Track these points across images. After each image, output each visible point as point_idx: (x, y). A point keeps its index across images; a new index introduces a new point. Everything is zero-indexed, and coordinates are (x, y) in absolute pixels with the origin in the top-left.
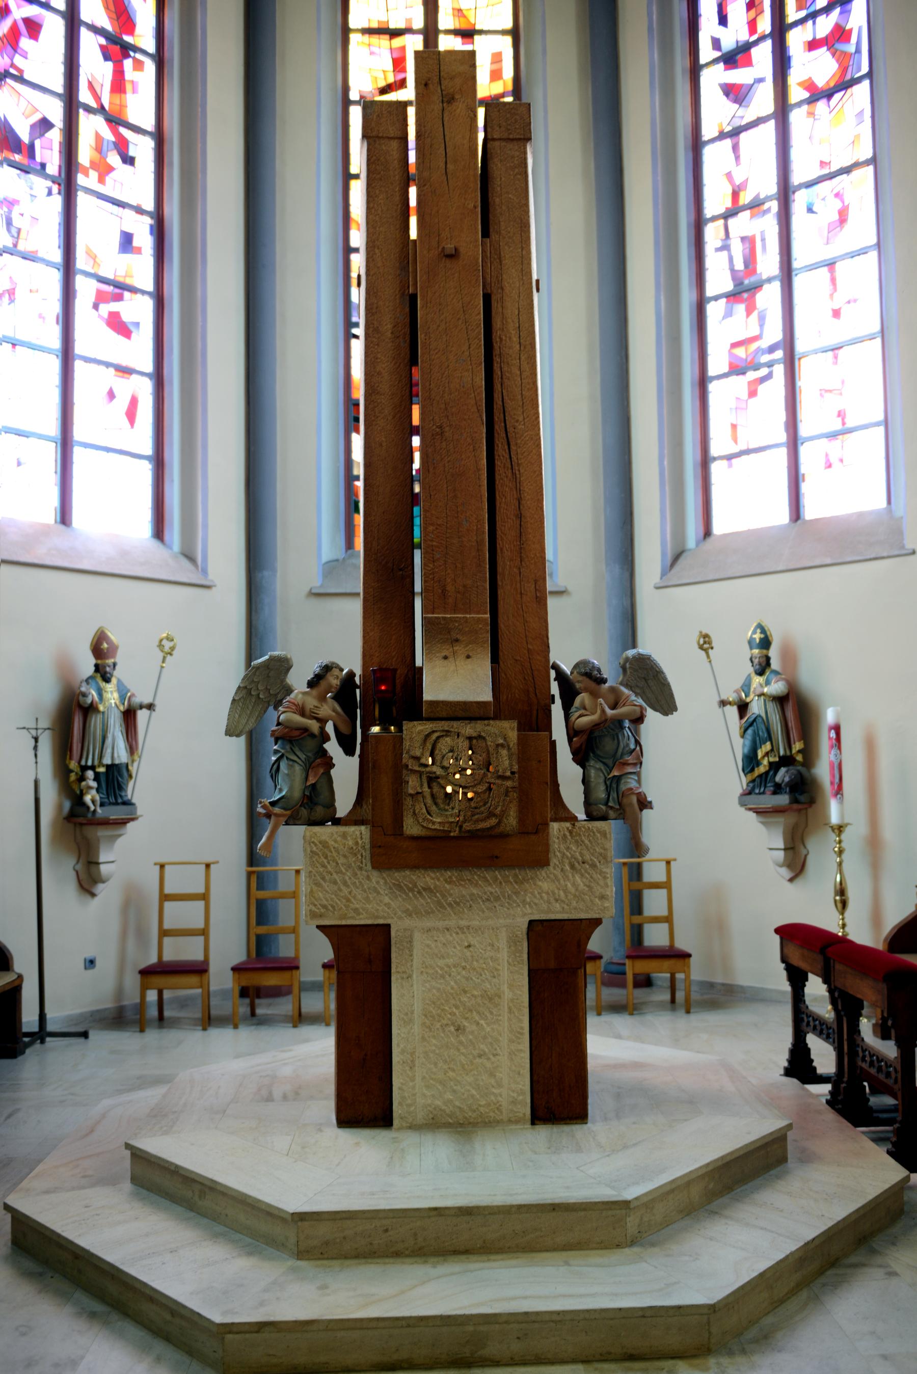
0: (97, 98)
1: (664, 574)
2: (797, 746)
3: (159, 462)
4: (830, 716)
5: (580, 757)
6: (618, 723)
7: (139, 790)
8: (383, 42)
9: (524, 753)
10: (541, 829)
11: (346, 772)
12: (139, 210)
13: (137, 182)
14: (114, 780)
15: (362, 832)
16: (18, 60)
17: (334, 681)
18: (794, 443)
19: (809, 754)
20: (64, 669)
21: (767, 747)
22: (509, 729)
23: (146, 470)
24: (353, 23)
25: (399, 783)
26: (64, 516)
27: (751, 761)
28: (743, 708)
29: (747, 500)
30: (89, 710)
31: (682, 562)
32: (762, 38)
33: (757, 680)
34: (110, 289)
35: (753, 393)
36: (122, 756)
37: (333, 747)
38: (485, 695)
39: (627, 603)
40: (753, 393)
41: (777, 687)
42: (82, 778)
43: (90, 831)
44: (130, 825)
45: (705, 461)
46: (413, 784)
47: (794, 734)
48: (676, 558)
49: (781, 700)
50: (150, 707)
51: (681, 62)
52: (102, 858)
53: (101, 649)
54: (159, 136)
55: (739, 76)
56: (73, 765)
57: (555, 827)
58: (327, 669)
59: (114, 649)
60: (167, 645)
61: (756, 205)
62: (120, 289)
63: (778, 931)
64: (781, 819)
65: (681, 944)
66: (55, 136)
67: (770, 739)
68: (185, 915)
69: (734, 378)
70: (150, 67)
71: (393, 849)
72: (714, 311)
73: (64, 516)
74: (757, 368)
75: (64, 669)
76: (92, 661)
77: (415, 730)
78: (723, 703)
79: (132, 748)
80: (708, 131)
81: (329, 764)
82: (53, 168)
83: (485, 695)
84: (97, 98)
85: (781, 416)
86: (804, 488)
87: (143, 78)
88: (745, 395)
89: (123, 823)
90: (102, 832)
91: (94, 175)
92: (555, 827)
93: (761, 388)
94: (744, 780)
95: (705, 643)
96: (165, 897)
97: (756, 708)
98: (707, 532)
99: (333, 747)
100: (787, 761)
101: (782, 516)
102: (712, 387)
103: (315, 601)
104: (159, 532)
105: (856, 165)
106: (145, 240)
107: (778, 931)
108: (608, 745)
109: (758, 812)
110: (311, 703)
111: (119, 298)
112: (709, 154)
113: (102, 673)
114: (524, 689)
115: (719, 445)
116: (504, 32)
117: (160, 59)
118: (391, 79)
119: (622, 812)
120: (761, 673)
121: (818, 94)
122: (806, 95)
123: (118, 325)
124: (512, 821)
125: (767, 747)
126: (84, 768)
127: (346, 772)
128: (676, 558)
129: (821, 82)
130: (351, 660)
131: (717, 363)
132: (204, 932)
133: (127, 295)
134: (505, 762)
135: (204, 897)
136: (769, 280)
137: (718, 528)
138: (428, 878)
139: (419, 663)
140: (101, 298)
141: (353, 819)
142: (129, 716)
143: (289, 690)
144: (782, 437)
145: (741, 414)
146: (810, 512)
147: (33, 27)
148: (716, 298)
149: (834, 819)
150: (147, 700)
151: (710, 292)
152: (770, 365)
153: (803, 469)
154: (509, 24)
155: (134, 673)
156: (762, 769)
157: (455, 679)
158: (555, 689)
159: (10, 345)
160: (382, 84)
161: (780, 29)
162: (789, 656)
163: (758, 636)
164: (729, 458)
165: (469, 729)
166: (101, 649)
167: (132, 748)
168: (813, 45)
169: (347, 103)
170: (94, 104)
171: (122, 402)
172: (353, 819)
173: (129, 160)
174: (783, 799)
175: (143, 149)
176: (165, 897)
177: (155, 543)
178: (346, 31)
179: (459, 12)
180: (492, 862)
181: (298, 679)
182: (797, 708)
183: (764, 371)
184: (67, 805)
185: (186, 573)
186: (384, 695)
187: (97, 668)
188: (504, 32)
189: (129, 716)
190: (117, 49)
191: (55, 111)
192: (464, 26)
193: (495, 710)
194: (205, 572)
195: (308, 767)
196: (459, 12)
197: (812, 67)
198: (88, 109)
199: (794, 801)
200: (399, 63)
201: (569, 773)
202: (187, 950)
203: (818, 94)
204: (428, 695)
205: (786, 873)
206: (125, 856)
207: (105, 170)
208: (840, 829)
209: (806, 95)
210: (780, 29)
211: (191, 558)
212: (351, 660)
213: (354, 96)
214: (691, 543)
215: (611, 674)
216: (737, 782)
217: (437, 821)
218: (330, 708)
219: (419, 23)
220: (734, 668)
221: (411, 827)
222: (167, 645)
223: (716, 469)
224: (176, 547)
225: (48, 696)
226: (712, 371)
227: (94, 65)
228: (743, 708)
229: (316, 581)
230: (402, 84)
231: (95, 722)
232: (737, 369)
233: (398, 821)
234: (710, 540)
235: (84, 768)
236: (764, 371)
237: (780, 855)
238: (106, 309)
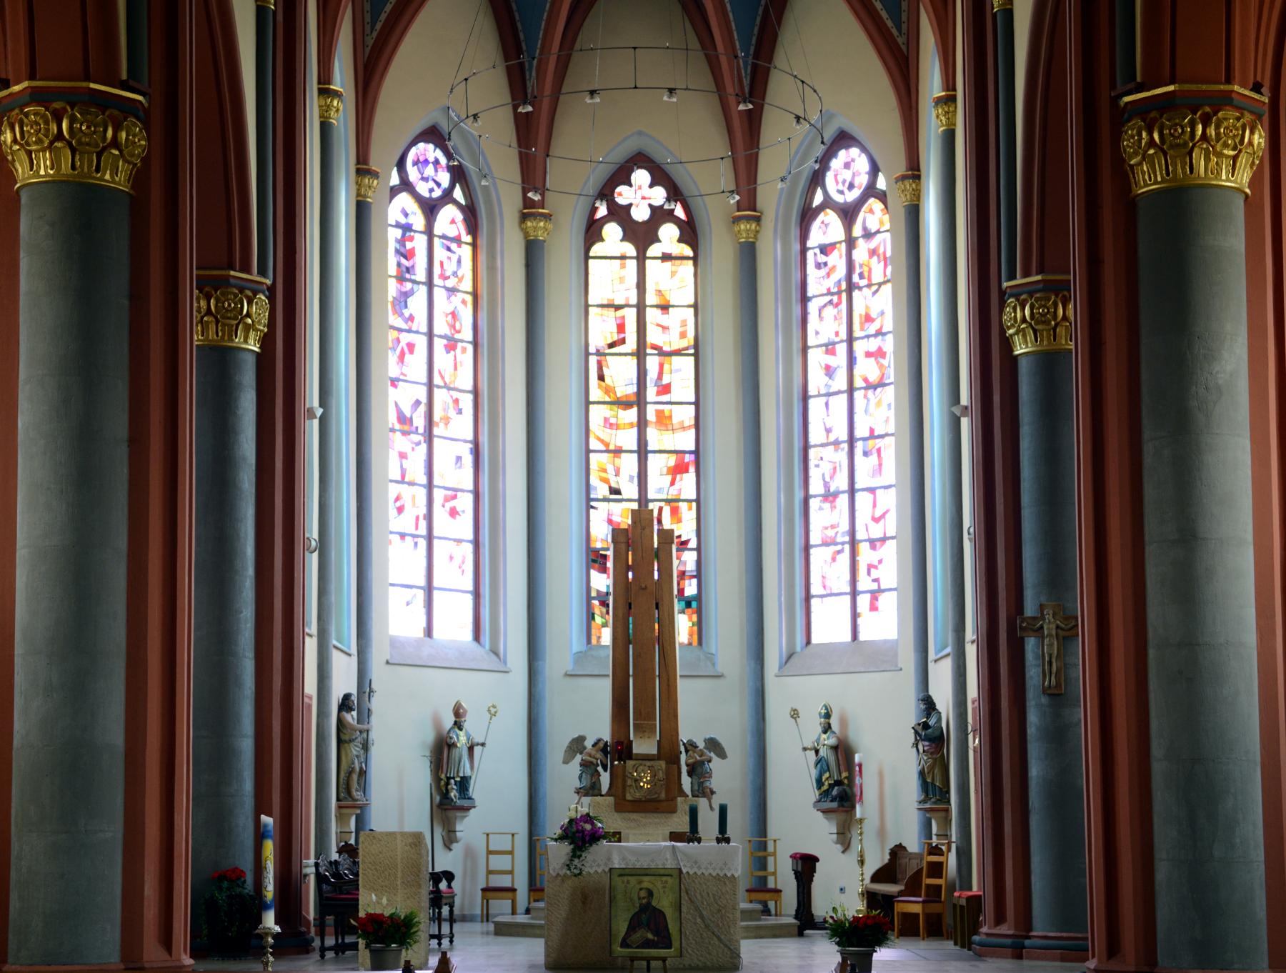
0: (443, 378)
1: (780, 668)
2: (844, 774)
3: (477, 594)
4: (857, 758)
5: (690, 774)
6: (702, 763)
7: (475, 790)
8: (610, 313)
9: (668, 772)
10: (674, 799)
11: (605, 778)
12: (465, 441)
13: (463, 426)
14: (464, 784)
15: (611, 799)
16: (405, 370)
17: (601, 745)
18: (854, 594)
19: (851, 778)
20: (437, 723)
21: (827, 775)
22: (662, 764)
23: (469, 600)
24: (592, 300)
25: (624, 781)
26: (429, 632)
27: (819, 783)
28: (817, 752)
29: (829, 624)
30: (452, 746)
31: (792, 660)
32: (842, 341)
33: (824, 736)
34: (450, 493)
35: (834, 559)
36: (468, 772)
37: (600, 769)
38: (655, 752)
39: (759, 684)
40: (834, 559)
41: (832, 741)
42: (447, 784)
43: (451, 814)
44: (472, 811)
45: (808, 598)
46: (629, 782)
47: (842, 768)
48: (790, 657)
49: (835, 748)
50: (483, 745)
51: (796, 345)
52: (458, 828)
53: (458, 712)
54: (476, 392)
55: (831, 360)
56: (443, 776)
57: (679, 799)
58: (599, 740)
59: (465, 711)
60: (493, 710)
61: (836, 443)
62: (454, 493)
63: (794, 857)
64: (833, 815)
65: (779, 887)
66: (422, 409)
67: (829, 770)
68: (500, 863)
69: (824, 548)
70: (470, 348)
71: (622, 805)
72: (814, 504)
73: (429, 632)
74: (836, 544)
75: (437, 723)
76: (453, 719)
77: (630, 763)
78: (805, 749)
79: (472, 768)
80: (812, 390)
81: (599, 775)
82: (421, 430)
83: (655, 752)
84: (443, 378)
85: (847, 577)
86: (859, 621)
87: (467, 358)
88: (829, 560)
89: (468, 809)
90: (459, 814)
91: (442, 425)
92: (679, 799)
93: (838, 557)
94: (817, 793)
95: (795, 714)
96: (489, 852)
97: (822, 753)
98: (808, 642)
99: (600, 769)
100: (838, 783)
101: (847, 637)
102: (812, 551)
103: (568, 679)
104: (477, 636)
105: (887, 435)
106: (468, 460)
107: (794, 857)
108: (699, 770)
109: (824, 812)
110: (593, 753)
111: (455, 497)
112: (812, 403)
113: (458, 725)
114: (669, 752)
115: (815, 589)
116: (689, 306)
117: (475, 344)
118: (615, 338)
119: (704, 795)
120: (825, 732)
121: (871, 386)
122: (864, 385)
123: (454, 513)
124: (663, 796)
125: (827, 775)
126: (449, 779)
127: (605, 778)
128: (790, 657)
129: (871, 380)
130: (607, 736)
131: (815, 538)
132: (511, 872)
133: (459, 494)
134: (661, 775)
135: (511, 853)
136: (843, 492)
137: (815, 639)
138: (634, 816)
139: (632, 737)
140: (447, 499)
141: (608, 794)
142: (471, 749)
143: (585, 748)
144: (848, 589)
145: (828, 569)
146: (863, 636)
147: (411, 347)
148: (815, 496)
149: (858, 815)
150: (481, 741)
151: (812, 491)
152: (843, 543)
153: (859, 610)
154: (692, 302)
155: (474, 727)
156: (825, 787)
157: (644, 746)
158: (682, 749)
159: (398, 537)
160: (610, 341)
161: (850, 340)
162: (844, 722)
163: (823, 711)
164: (822, 596)
165: (648, 763)
166: (458, 712)
167: (472, 768)
168: (868, 354)
169: (587, 354)
170: (442, 384)
171: (457, 560)
172: (608, 794)
173: (460, 412)
174: (835, 805)
175: (467, 401)
176: (489, 852)
177: (475, 644)
178: (587, 306)
179: (659, 292)
180: (656, 811)
181: (589, 744)
182: (844, 751)
183: (839, 547)
184: (437, 799)
185: (491, 662)
186: (619, 750)
187: (455, 723)
188: (689, 306)
189: (471, 749)
190: (451, 345)
191: (422, 394)
192: (663, 303)
193: (659, 757)
194: (505, 663)
195: (592, 776)
196: (659, 292)
197: (866, 369)
198: (439, 387)
199: (841, 805)
200: (621, 328)
201: (686, 782)
202: (505, 881)
203: (871, 386)
204: (635, 751)
205: (839, 847)
206: (468, 827)
207: (447, 420)
208: (861, 820)
209: (864, 385)
210: (850, 340)
211: (496, 654)
212: (607, 736)
213: (592, 350)
214: (798, 649)
215: (701, 745)
216: (813, 794)
217: (638, 795)
218: (600, 755)
219: (634, 301)
220: (811, 729)
221: (629, 797)
222: (493, 710)
223: (814, 602)
224: (487, 647)
225: (430, 737)
226: (812, 542)
227: (443, 360)
228: (817, 752)
229: (569, 666)
230: (623, 341)
231: (455, 752)
232: (825, 543)
233: (624, 796)
234: (810, 647)
235: (449, 779)
236: (839, 547)
237: (835, 836)
238: (449, 505)
